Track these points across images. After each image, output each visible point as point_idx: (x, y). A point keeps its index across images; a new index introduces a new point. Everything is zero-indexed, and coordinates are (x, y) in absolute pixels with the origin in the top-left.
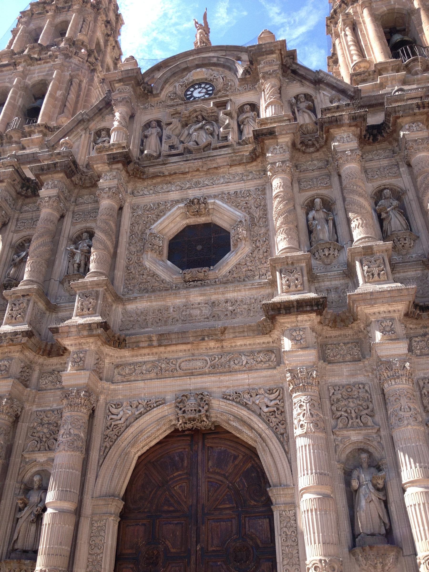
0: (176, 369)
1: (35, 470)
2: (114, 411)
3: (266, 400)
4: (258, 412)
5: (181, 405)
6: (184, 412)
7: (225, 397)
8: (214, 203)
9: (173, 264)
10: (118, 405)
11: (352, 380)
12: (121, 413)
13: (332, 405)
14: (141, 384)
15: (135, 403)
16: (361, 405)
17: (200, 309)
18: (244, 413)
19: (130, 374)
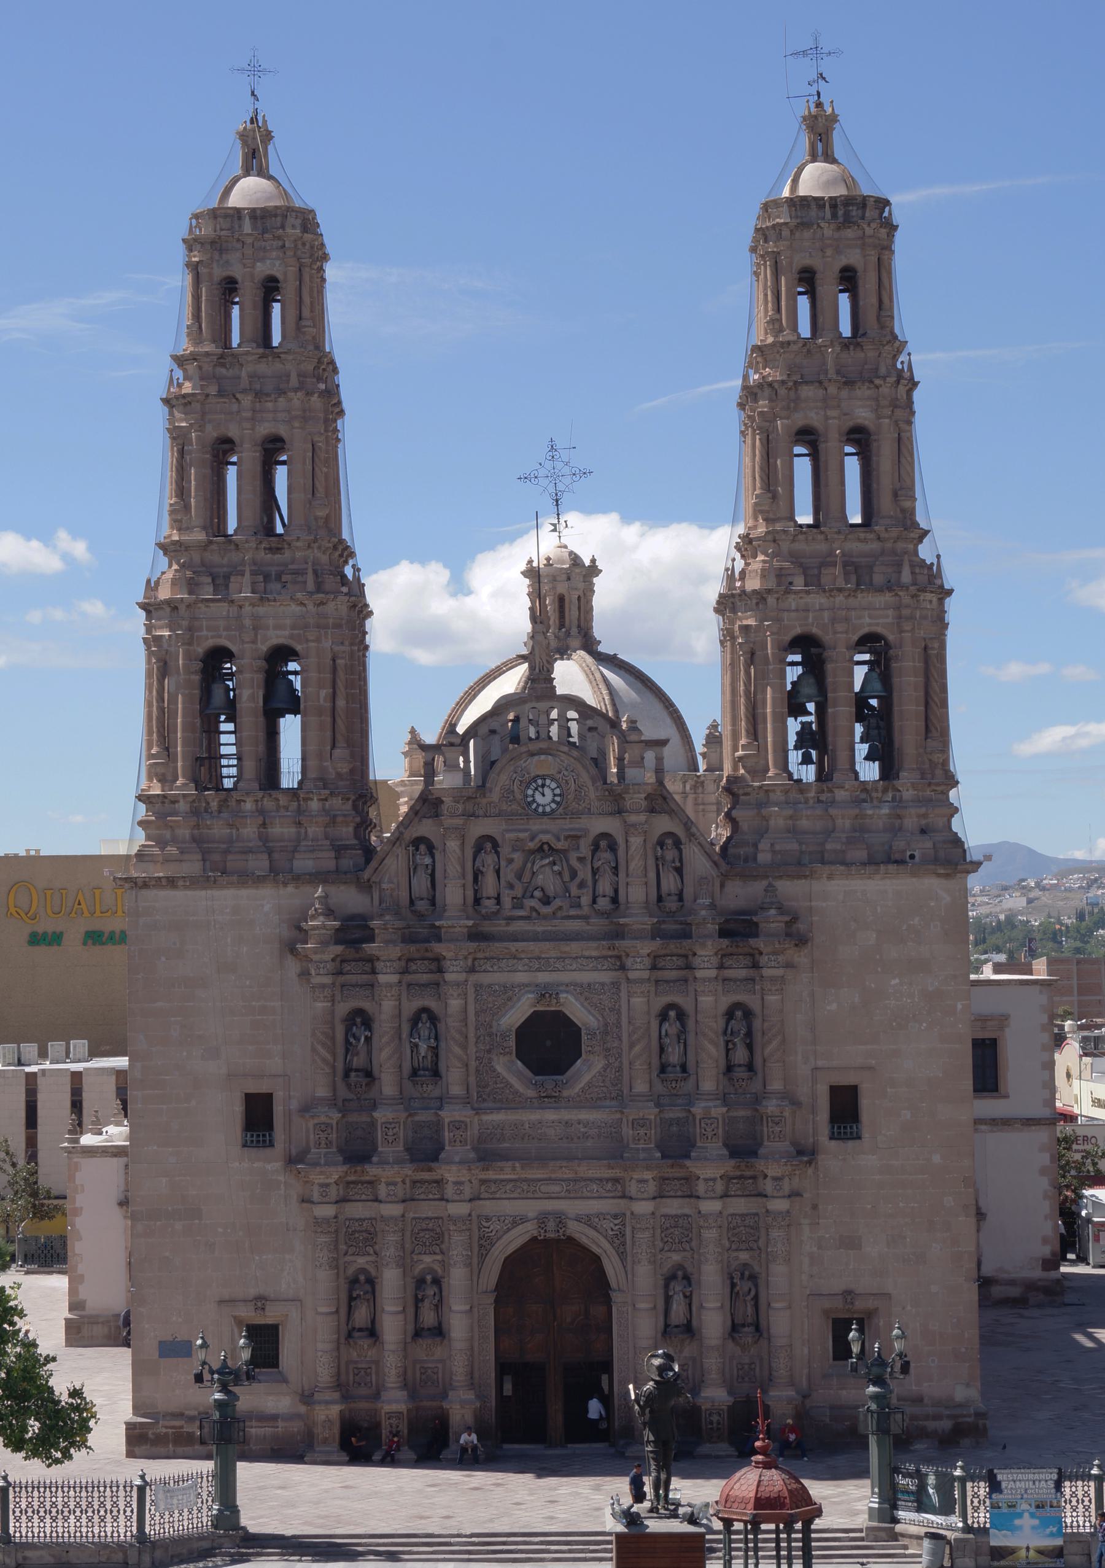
0: (535, 1191)
1: (422, 1266)
2: (486, 1224)
3: (612, 1225)
4: (604, 1234)
5: (543, 1226)
6: (545, 1231)
7: (578, 1219)
8: (566, 998)
9: (525, 1068)
10: (488, 1219)
11: (679, 1212)
12: (492, 1227)
13: (662, 1232)
14: (506, 1202)
15: (503, 1218)
16: (683, 1234)
17: (555, 1130)
18: (592, 1233)
19: (495, 1192)
